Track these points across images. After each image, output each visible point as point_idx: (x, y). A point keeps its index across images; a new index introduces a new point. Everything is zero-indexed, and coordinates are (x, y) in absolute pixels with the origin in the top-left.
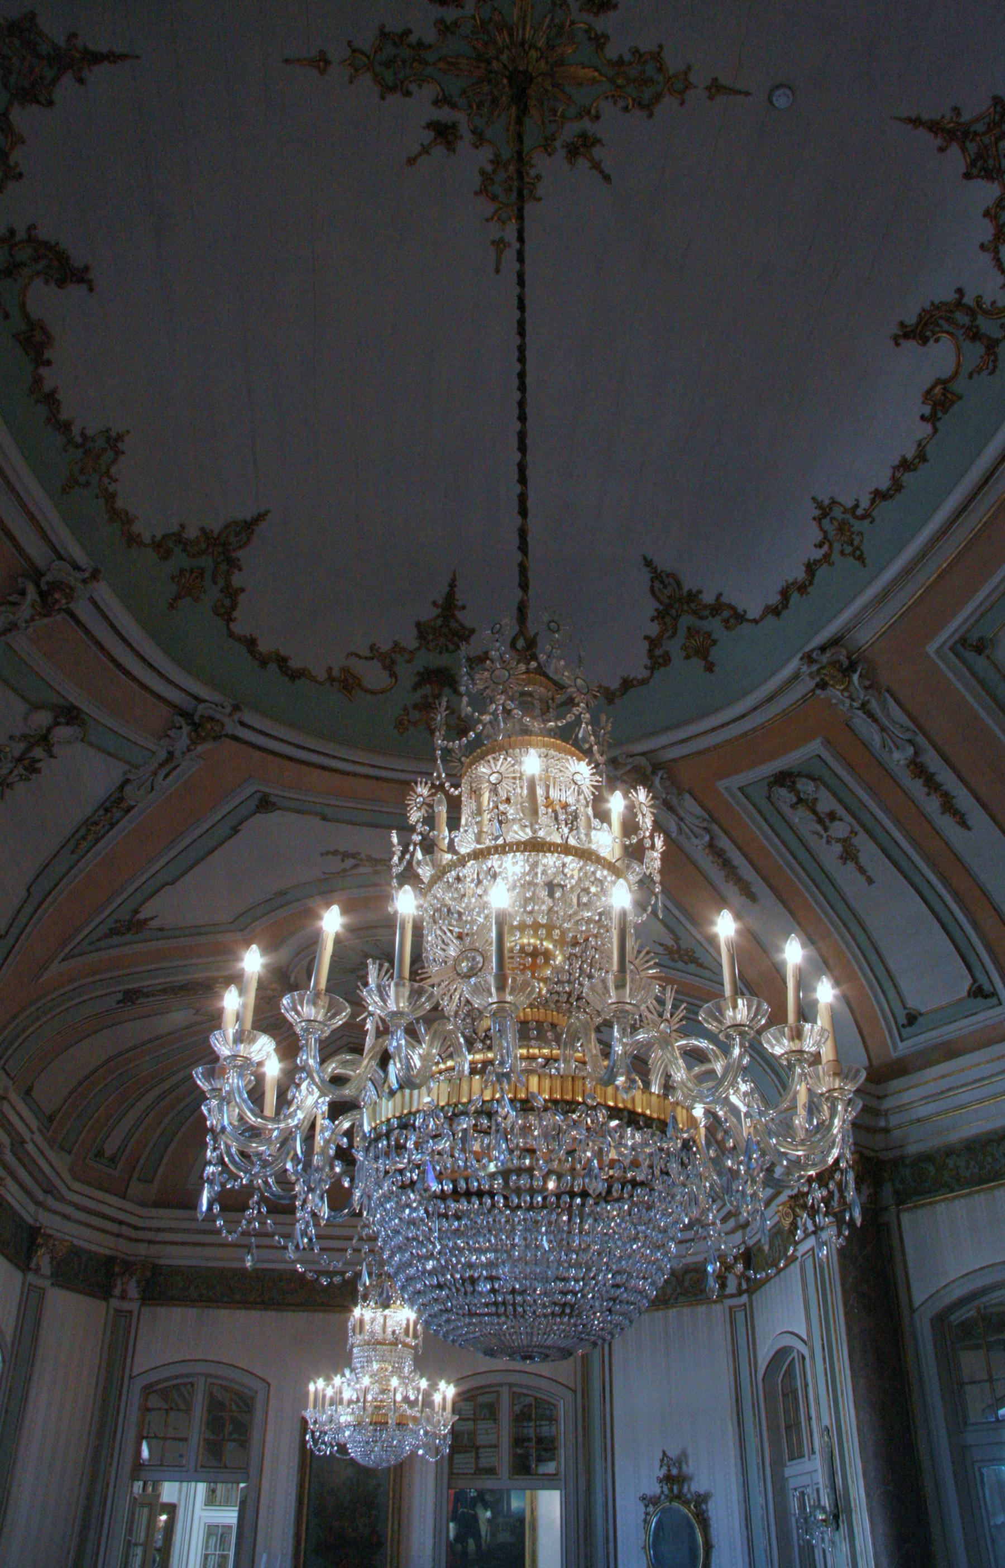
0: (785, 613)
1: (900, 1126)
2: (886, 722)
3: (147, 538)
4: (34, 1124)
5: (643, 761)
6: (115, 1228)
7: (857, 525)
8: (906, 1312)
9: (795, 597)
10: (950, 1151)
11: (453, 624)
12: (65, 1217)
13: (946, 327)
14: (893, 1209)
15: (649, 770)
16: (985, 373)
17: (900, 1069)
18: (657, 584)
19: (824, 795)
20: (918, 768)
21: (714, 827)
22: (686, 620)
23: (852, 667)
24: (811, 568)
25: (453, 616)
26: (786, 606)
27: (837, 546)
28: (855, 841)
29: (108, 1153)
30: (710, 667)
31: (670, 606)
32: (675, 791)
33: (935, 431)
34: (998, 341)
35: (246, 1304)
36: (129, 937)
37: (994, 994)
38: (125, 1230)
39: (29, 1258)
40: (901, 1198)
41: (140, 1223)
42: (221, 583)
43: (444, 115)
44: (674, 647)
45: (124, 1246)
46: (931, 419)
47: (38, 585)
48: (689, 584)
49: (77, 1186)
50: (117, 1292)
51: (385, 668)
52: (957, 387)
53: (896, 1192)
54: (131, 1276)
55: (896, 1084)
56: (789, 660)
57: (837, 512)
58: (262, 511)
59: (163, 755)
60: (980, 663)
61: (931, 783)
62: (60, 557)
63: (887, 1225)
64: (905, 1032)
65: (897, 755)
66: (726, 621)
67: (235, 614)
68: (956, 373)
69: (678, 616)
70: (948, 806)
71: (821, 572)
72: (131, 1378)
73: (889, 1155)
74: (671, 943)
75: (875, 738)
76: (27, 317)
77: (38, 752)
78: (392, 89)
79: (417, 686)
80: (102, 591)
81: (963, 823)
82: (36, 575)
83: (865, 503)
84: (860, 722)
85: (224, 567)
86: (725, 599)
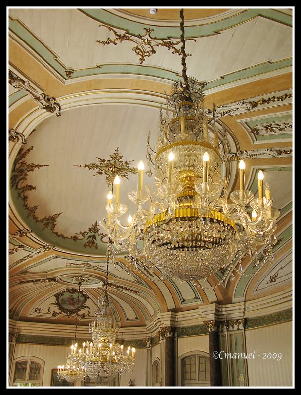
3: (39, 220)
10: (188, 328)
17: (181, 310)
35: (40, 344)
40: (179, 336)
43: (100, 171)
53: (178, 334)
55: (180, 313)
64: (183, 303)
79: (88, 239)
82: (20, 230)
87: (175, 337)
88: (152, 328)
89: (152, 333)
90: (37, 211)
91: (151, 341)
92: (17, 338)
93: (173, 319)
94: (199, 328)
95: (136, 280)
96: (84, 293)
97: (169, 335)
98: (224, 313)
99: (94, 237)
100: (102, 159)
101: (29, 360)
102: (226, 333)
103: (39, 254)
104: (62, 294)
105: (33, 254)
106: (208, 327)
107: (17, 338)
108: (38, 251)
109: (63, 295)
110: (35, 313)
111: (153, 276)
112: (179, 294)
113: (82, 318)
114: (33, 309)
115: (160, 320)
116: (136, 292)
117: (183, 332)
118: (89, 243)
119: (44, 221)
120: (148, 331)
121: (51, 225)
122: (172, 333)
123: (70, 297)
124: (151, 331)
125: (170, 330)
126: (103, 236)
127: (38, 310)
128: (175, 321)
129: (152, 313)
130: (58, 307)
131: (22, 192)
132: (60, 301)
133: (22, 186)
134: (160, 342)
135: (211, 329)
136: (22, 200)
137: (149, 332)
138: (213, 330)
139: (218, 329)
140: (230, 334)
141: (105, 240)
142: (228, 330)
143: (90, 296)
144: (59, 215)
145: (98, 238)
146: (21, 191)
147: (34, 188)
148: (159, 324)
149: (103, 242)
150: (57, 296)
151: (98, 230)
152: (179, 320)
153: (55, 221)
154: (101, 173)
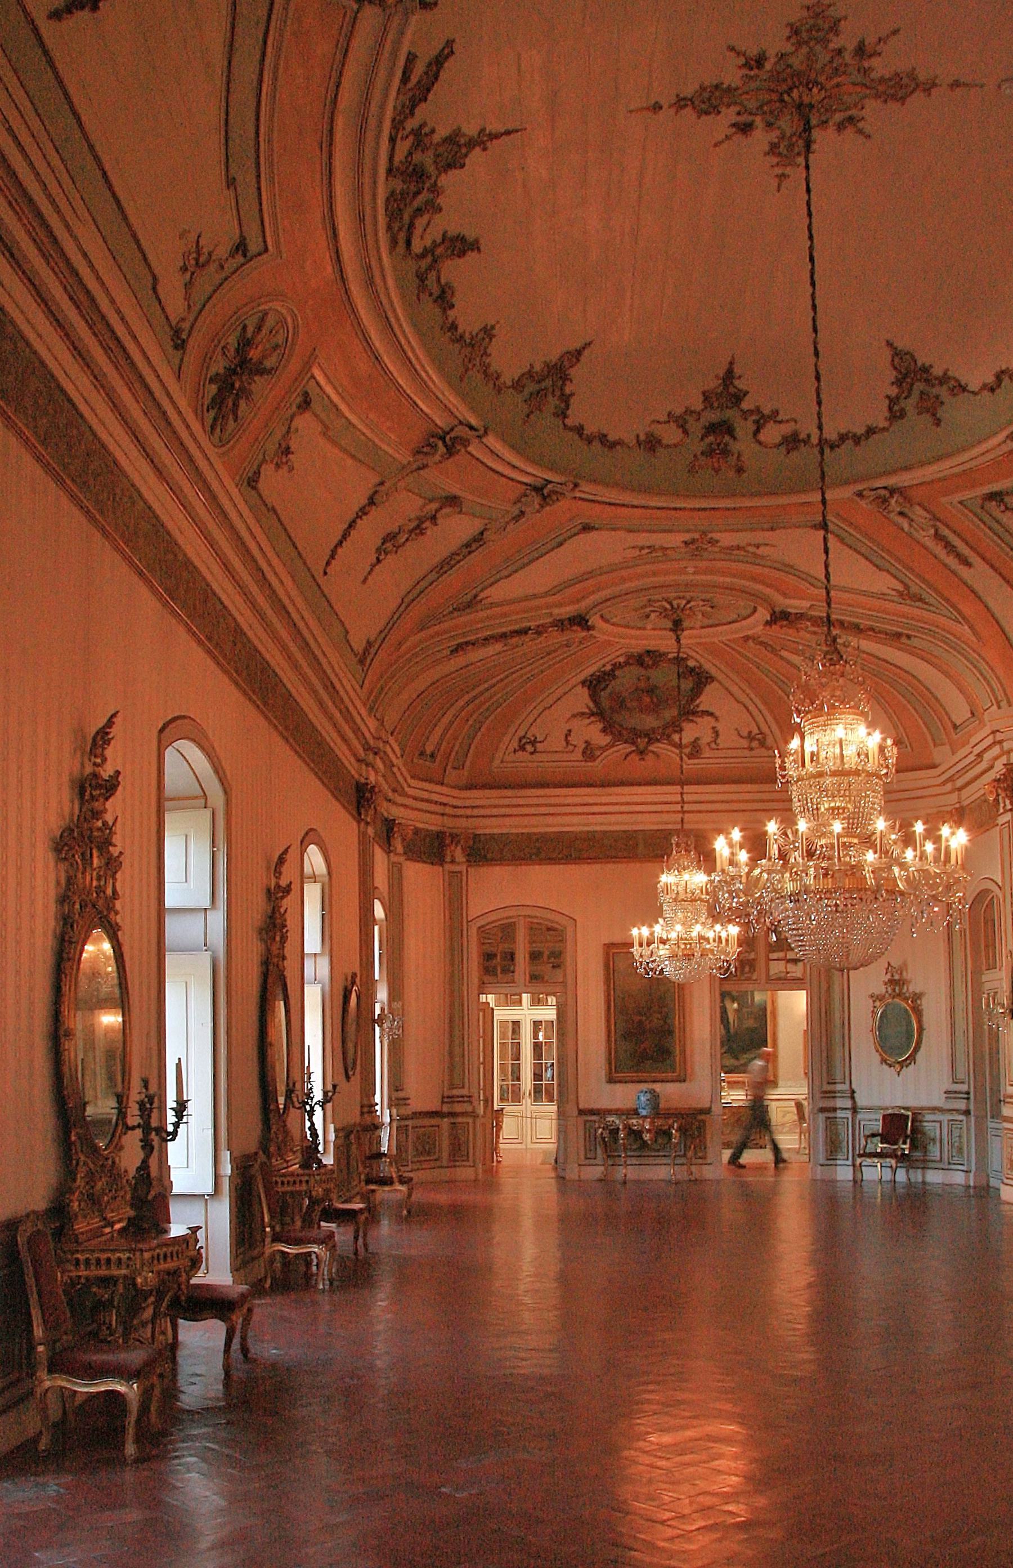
0: (998, 391)
5: (883, 492)
6: (439, 809)
12: (405, 806)
15: (888, 495)
21: (938, 523)
22: (919, 386)
26: (999, 386)
29: (428, 752)
30: (938, 422)
31: (905, 376)
32: (908, 505)
35: (551, 861)
38: (448, 810)
41: (459, 803)
43: (744, 118)
44: (909, 405)
45: (449, 822)
47: (444, 442)
49: (413, 782)
50: (448, 859)
51: (678, 426)
54: (456, 845)
58: (588, 340)
62: (461, 423)
66: (952, 390)
67: (569, 412)
69: (912, 385)
72: (468, 922)
77: (427, 524)
78: (707, 113)
79: (702, 439)
80: (490, 440)
86: (950, 373)
88: (965, 770)
90: (495, 348)
92: (471, 848)
95: (900, 588)
96: (691, 663)
100: (753, 52)
109: (614, 677)
111: (969, 565)
113: (691, 756)
115: (999, 737)
116: (898, 635)
118: (709, 453)
123: (642, 685)
126: (761, 420)
127: (527, 744)
129: (960, 711)
130: (601, 726)
131: (430, 268)
132: (605, 703)
133: (428, 243)
136: (435, 301)
141: (772, 433)
143: (713, 671)
144: (579, 353)
145: (744, 428)
146: (425, 263)
147: (475, 246)
148: (996, 750)
149: (760, 443)
151: (738, 398)
153: (565, 378)
154: (745, 128)
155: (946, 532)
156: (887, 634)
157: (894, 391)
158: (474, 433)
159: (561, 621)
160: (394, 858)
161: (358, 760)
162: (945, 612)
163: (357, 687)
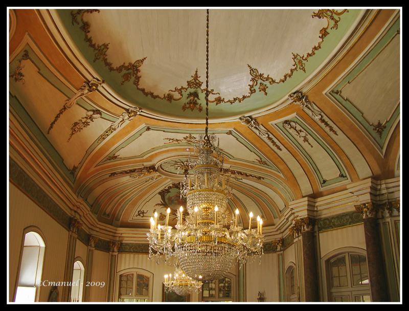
1: (320, 210)
2: (312, 109)
3: (115, 68)
4: (89, 209)
7: (304, 62)
8: (319, 258)
9: (288, 78)
10: (333, 218)
11: (197, 81)
13: (325, 15)
14: (317, 232)
16: (335, 29)
17: (320, 195)
18: (252, 72)
19: (297, 125)
20: (323, 121)
23: (303, 97)
24: (292, 71)
25: (197, 79)
26: (286, 79)
27: (298, 66)
28: (307, 137)
29: (107, 213)
30: (266, 94)
33: (323, 41)
34: (338, 21)
36: (112, 160)
37: (346, 176)
39: (88, 243)
40: (320, 229)
42: (135, 76)
46: (322, 37)
48: (260, 72)
49: (100, 223)
50: (112, 250)
52: (328, 31)
53: (318, 227)
55: (319, 199)
56: (285, 95)
57: (298, 57)
58: (145, 57)
59: (122, 120)
60: (337, 96)
61: (327, 124)
62: (94, 78)
63: (316, 236)
64: (324, 185)
65: (316, 117)
66: (270, 82)
68: (328, 27)
70: (331, 129)
71: (295, 72)
73: (318, 217)
74: (259, 159)
75: (310, 113)
76: (83, 22)
77: (89, 121)
79: (188, 98)
81: (336, 133)
82: (88, 82)
83: (305, 56)
84: (306, 110)
85: (135, 72)
87: (315, 232)
89: (282, 233)
91: (283, 244)
92: (120, 248)
93: (311, 208)
94: (348, 217)
97: (306, 229)
98: (384, 192)
99: (195, 95)
101: (134, 271)
102: (388, 220)
103: (124, 125)
104: (167, 191)
105: (116, 124)
106: (362, 213)
107: (120, 248)
108: (121, 119)
110: (139, 217)
111: (281, 150)
112: (318, 173)
114: (135, 212)
115: (293, 211)
116: (260, 178)
117: (325, 223)
118: (190, 103)
119: (121, 70)
120: (277, 231)
121: (133, 78)
122: (310, 227)
124: (282, 230)
125: (307, 222)
128: (314, 211)
132: (166, 201)
134: (295, 241)
135: (367, 215)
137: (279, 232)
138: (369, 216)
139: (376, 215)
140: (395, 221)
142: (391, 216)
145: (202, 96)
150: (162, 194)
152: (319, 208)
153: (138, 71)
155: (271, 136)
156: (255, 177)
157: (251, 83)
158: (99, 82)
159: (147, 168)
160: (89, 247)
161: (71, 209)
162: (274, 168)
163: (72, 184)
